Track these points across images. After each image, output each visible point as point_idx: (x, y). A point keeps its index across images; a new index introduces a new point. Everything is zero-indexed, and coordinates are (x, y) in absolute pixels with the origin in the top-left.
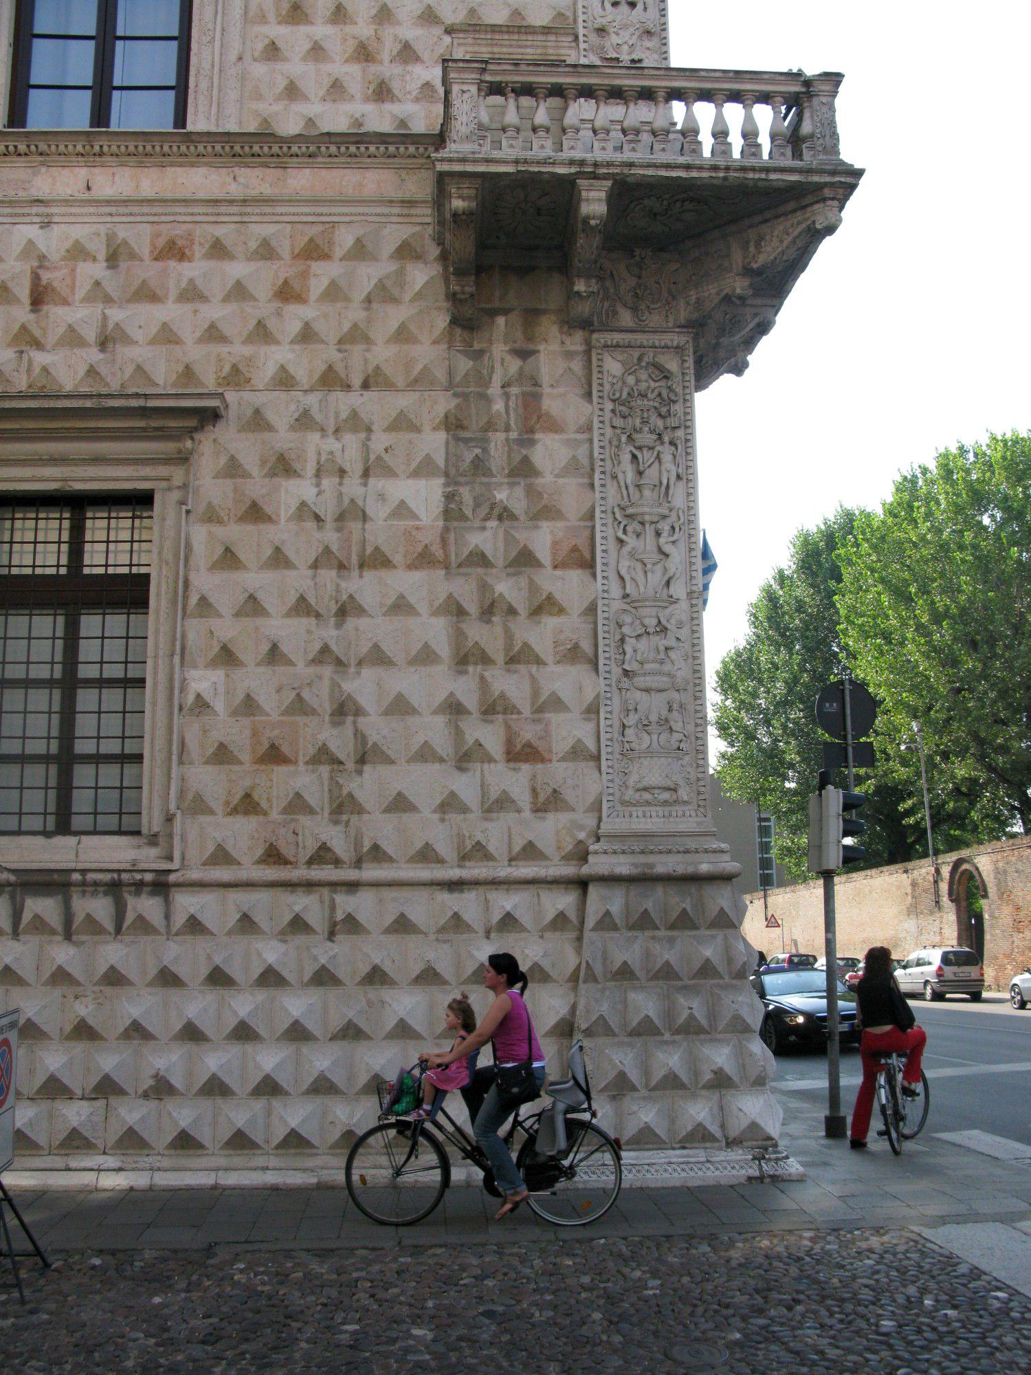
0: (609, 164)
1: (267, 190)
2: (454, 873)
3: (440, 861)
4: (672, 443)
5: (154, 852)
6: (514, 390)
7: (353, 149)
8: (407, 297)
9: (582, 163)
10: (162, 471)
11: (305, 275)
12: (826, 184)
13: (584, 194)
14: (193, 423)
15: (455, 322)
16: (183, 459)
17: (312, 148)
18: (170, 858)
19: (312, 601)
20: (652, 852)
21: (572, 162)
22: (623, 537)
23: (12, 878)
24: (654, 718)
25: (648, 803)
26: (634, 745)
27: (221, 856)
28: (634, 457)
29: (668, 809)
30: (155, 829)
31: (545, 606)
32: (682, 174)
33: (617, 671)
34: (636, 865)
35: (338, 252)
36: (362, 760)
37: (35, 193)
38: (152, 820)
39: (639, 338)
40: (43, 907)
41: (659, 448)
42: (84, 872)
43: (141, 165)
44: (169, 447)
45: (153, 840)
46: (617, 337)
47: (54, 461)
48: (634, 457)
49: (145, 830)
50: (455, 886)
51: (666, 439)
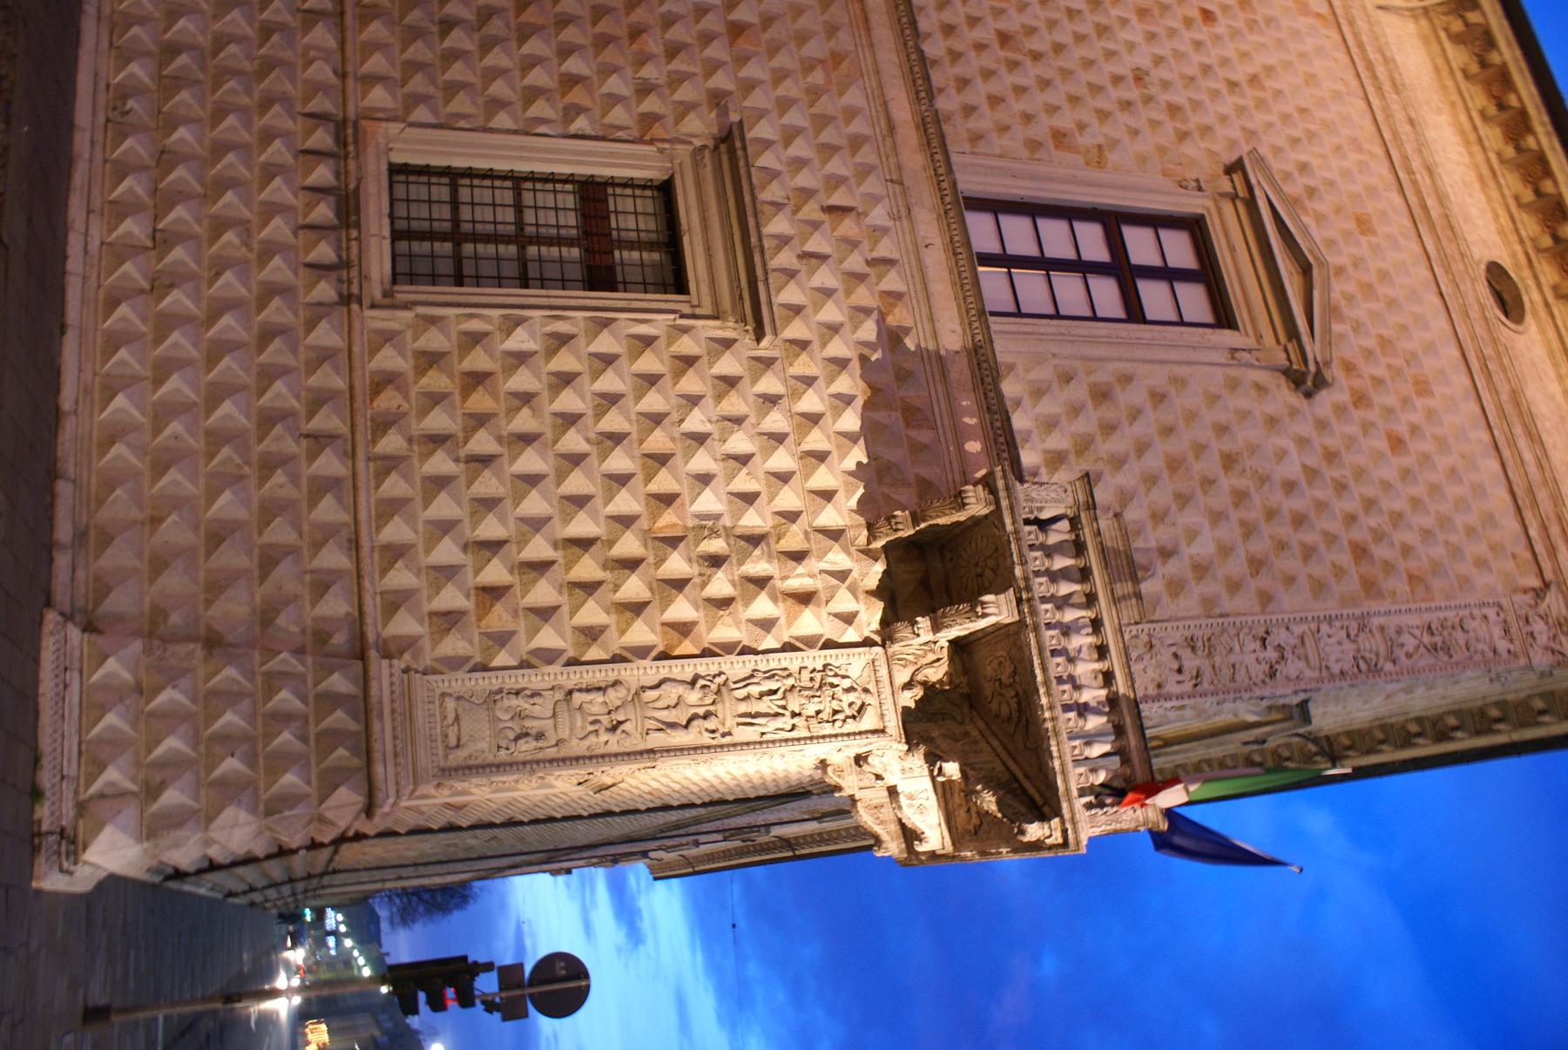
0: (1033, 612)
1: (954, 375)
4: (794, 727)
5: (378, 294)
7: (1002, 439)
8: (886, 490)
9: (1028, 589)
13: (1002, 596)
17: (995, 408)
18: (373, 306)
20: (393, 720)
21: (1026, 579)
22: (698, 685)
23: (352, 186)
24: (528, 723)
26: (499, 704)
28: (775, 692)
29: (439, 739)
30: (399, 296)
32: (1040, 678)
33: (570, 685)
34: (381, 702)
35: (913, 433)
37: (915, 210)
38: (405, 292)
39: (887, 690)
41: (788, 713)
42: (358, 239)
43: (954, 284)
44: (726, 303)
45: (386, 294)
46: (883, 672)
48: (775, 692)
49: (397, 288)
51: (796, 720)
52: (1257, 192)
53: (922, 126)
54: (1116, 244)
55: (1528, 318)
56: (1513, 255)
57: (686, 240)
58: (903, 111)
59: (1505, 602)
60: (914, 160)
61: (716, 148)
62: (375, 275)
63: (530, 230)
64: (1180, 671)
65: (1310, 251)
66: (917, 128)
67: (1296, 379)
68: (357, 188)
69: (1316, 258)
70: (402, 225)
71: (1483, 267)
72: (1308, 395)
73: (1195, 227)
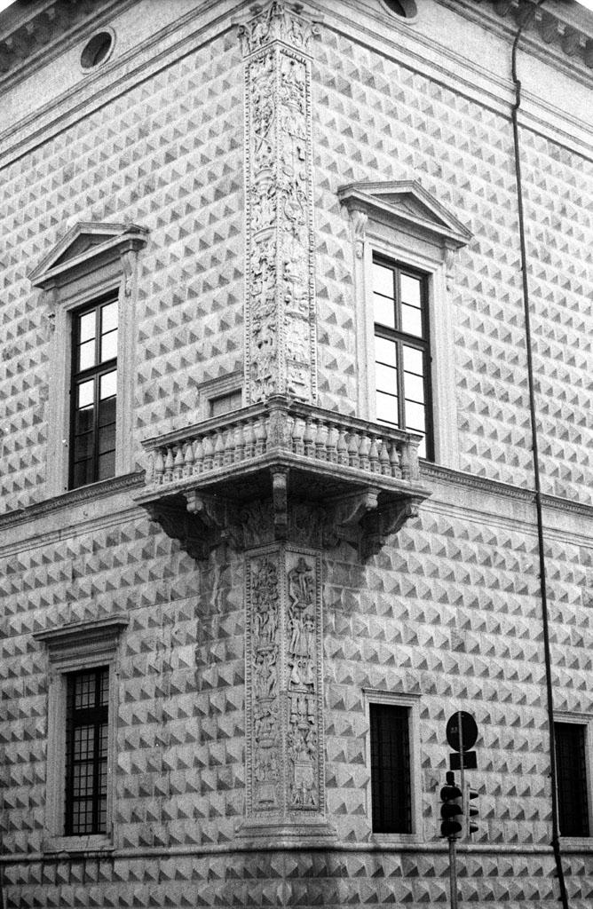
2: (197, 848)
3: (195, 843)
5: (108, 842)
6: (222, 590)
10: (109, 656)
11: (152, 543)
12: (268, 468)
14: (116, 630)
15: (197, 563)
16: (113, 649)
19: (154, 715)
23: (67, 855)
25: (263, 810)
27: (127, 844)
31: (229, 707)
32: (214, 481)
36: (171, 793)
40: (76, 870)
42: (88, 852)
44: (109, 643)
46: (252, 552)
47: (78, 656)
50: (200, 855)
52: (49, 276)
53: (36, 516)
54: (89, 373)
55: (106, 29)
56: (78, 41)
57: (87, 667)
58: (28, 529)
59: (246, 64)
60: (49, 523)
61: (50, 647)
62: (101, 843)
63: (91, 756)
64: (266, 342)
65: (74, 235)
66: (37, 518)
67: (139, 245)
68: (69, 853)
69: (77, 231)
70: (89, 829)
71: (88, 71)
72: (147, 231)
73: (76, 315)
